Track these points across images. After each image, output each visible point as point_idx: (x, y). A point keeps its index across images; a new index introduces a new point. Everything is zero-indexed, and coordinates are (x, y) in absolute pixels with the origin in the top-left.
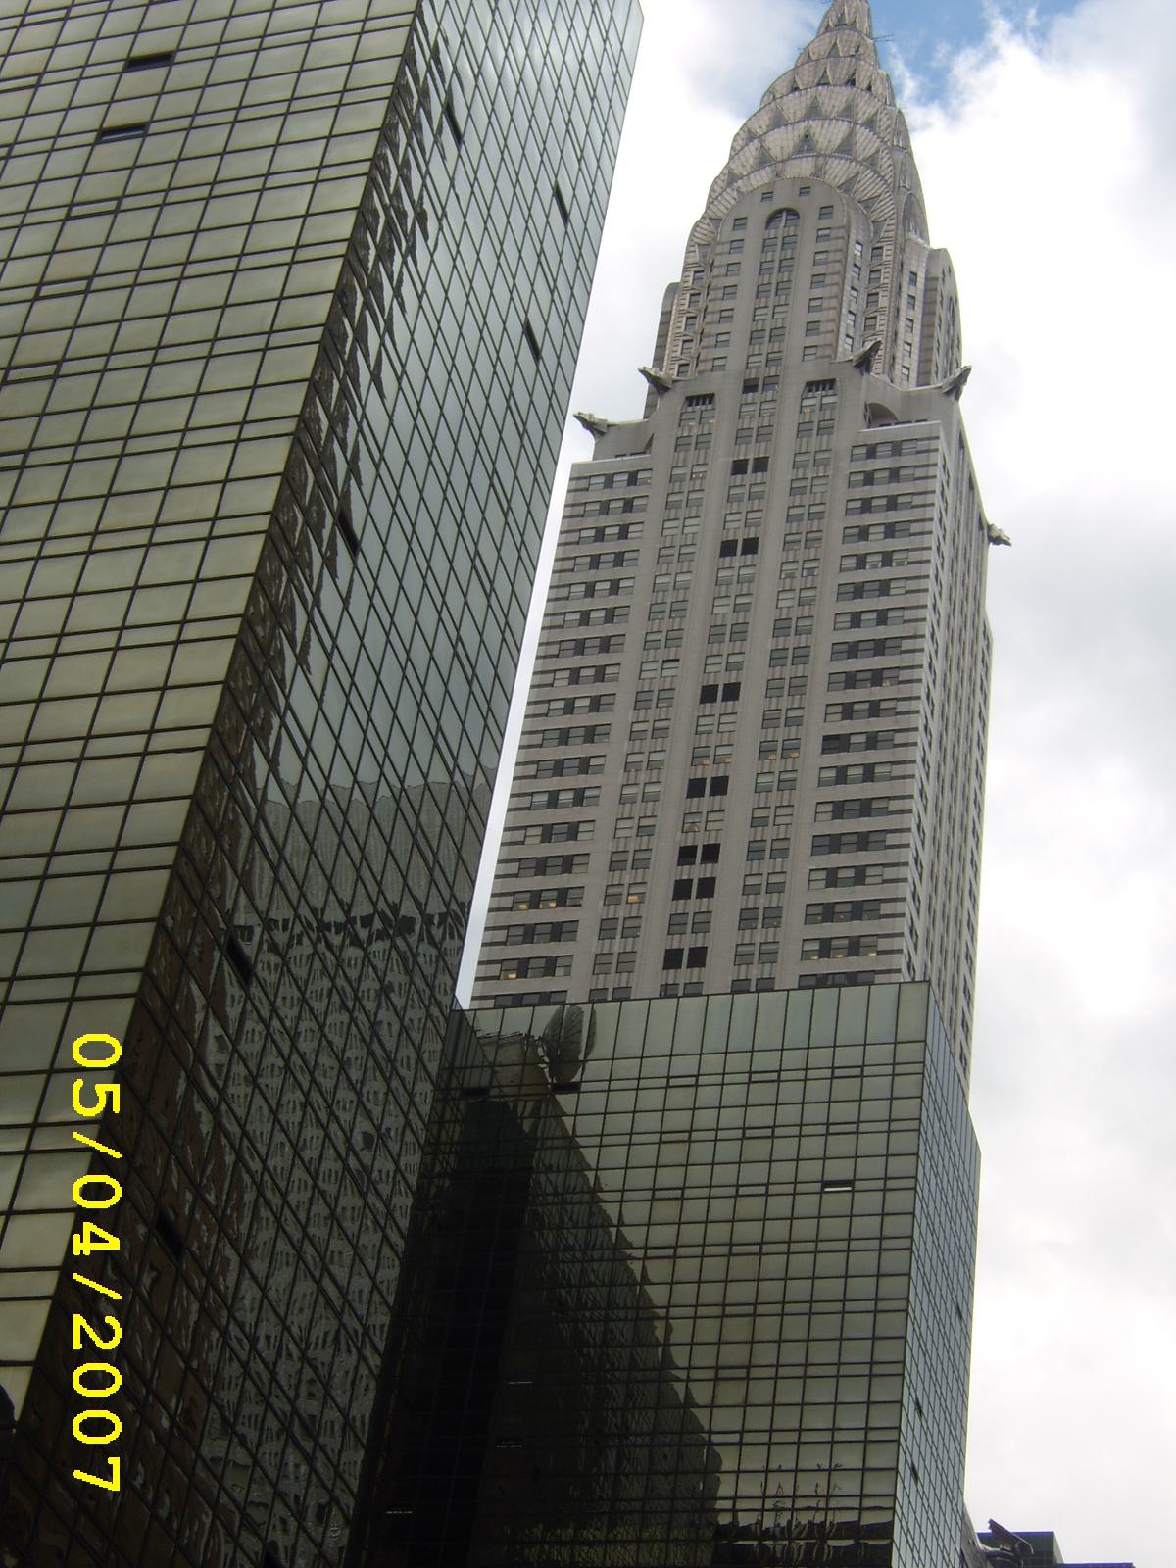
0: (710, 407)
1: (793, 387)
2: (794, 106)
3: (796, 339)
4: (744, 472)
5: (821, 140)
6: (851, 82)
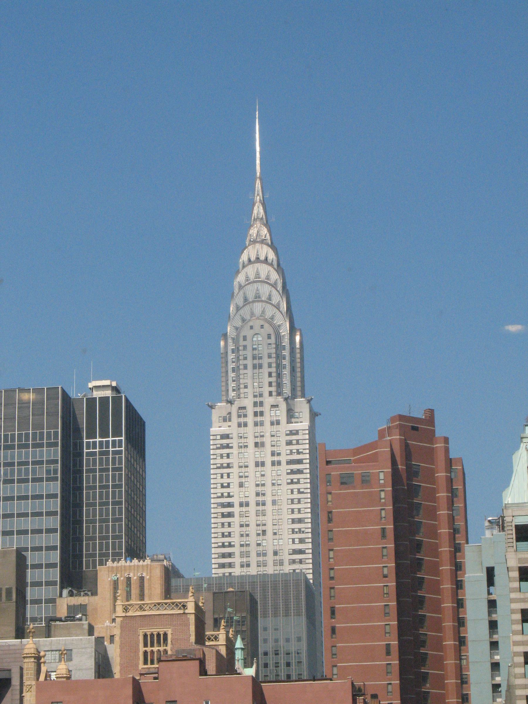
0: (245, 411)
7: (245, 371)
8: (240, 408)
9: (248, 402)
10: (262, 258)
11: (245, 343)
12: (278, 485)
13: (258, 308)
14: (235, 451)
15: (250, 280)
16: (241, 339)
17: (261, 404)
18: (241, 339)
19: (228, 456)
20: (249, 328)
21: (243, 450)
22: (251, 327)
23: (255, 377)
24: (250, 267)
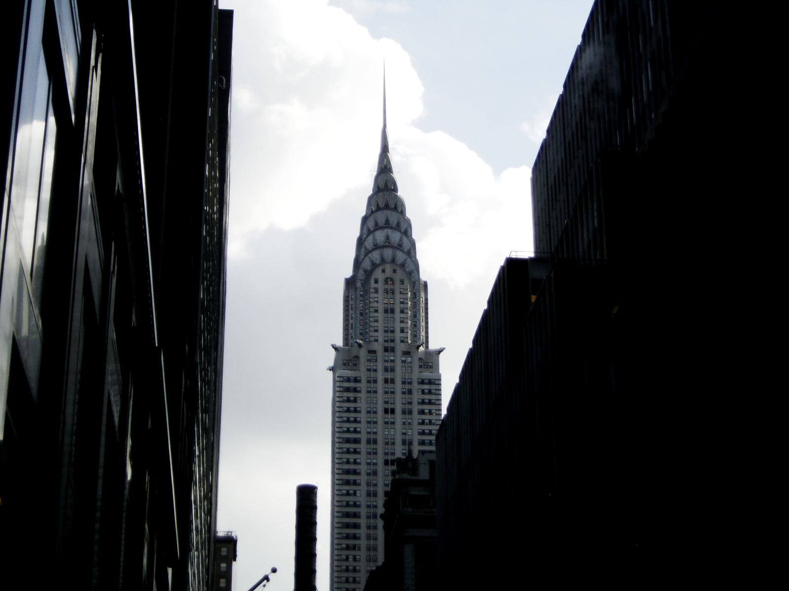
1: (399, 353)
3: (398, 335)
6: (395, 208)
7: (376, 314)
9: (378, 347)
11: (376, 286)
13: (388, 253)
14: (363, 395)
15: (378, 225)
16: (372, 281)
17: (393, 350)
18: (372, 281)
19: (355, 401)
20: (381, 271)
21: (372, 395)
22: (383, 271)
24: (378, 213)
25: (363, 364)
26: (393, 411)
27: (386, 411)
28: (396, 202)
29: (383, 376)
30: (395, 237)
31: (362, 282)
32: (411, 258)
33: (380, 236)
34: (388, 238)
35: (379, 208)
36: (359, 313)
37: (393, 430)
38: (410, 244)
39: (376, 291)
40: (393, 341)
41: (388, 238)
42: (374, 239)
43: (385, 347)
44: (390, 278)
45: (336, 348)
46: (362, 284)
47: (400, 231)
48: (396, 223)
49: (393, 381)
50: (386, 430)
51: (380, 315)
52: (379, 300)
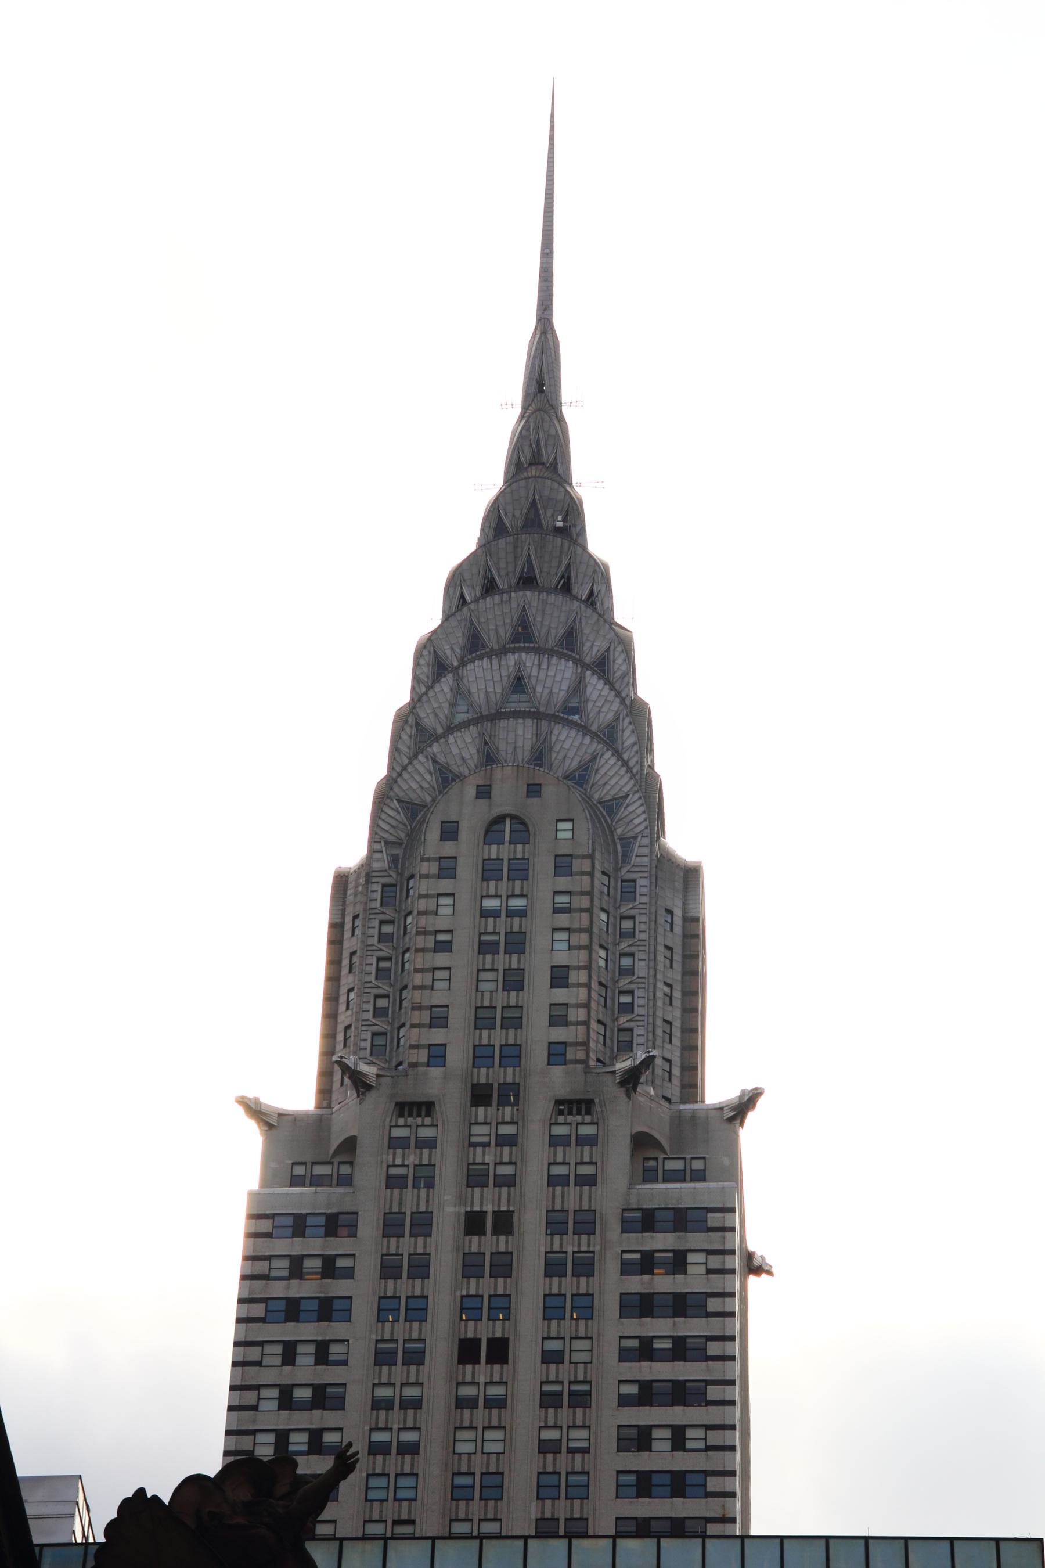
0: (428, 1121)
2: (496, 618)
3: (538, 1033)
4: (481, 1232)
5: (539, 689)
8: (405, 1108)
10: (548, 574)
11: (448, 849)
12: (571, 1451)
16: (433, 833)
18: (433, 833)
20: (471, 791)
22: (484, 792)
23: (483, 986)
25: (369, 1173)
26: (500, 1351)
27: (467, 1351)
28: (568, 566)
29: (460, 1201)
30: (553, 678)
31: (395, 851)
32: (618, 754)
33: (485, 679)
34: (519, 684)
35: (490, 588)
36: (373, 969)
37: (498, 1435)
38: (616, 705)
39: (447, 868)
40: (513, 1055)
41: (519, 684)
42: (460, 692)
43: (475, 1087)
44: (513, 817)
45: (255, 1110)
46: (394, 860)
47: (577, 662)
48: (561, 631)
49: (504, 1223)
50: (461, 1435)
51: (462, 960)
52: (455, 908)
